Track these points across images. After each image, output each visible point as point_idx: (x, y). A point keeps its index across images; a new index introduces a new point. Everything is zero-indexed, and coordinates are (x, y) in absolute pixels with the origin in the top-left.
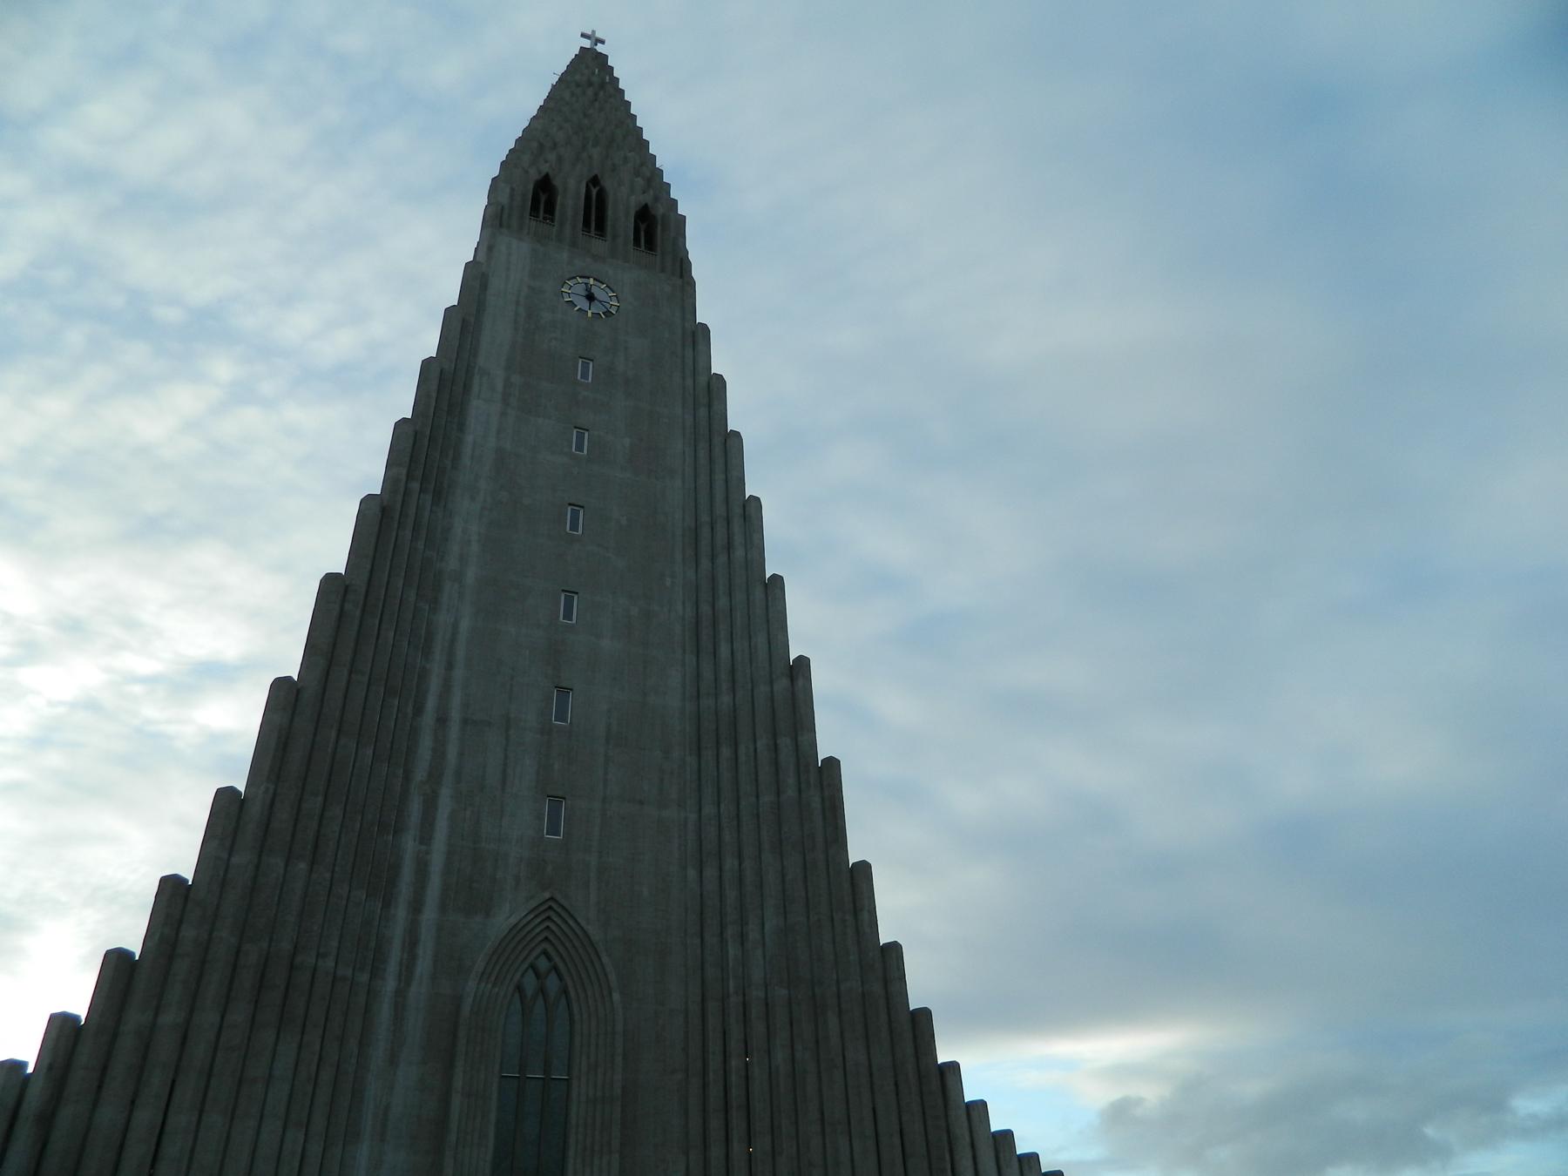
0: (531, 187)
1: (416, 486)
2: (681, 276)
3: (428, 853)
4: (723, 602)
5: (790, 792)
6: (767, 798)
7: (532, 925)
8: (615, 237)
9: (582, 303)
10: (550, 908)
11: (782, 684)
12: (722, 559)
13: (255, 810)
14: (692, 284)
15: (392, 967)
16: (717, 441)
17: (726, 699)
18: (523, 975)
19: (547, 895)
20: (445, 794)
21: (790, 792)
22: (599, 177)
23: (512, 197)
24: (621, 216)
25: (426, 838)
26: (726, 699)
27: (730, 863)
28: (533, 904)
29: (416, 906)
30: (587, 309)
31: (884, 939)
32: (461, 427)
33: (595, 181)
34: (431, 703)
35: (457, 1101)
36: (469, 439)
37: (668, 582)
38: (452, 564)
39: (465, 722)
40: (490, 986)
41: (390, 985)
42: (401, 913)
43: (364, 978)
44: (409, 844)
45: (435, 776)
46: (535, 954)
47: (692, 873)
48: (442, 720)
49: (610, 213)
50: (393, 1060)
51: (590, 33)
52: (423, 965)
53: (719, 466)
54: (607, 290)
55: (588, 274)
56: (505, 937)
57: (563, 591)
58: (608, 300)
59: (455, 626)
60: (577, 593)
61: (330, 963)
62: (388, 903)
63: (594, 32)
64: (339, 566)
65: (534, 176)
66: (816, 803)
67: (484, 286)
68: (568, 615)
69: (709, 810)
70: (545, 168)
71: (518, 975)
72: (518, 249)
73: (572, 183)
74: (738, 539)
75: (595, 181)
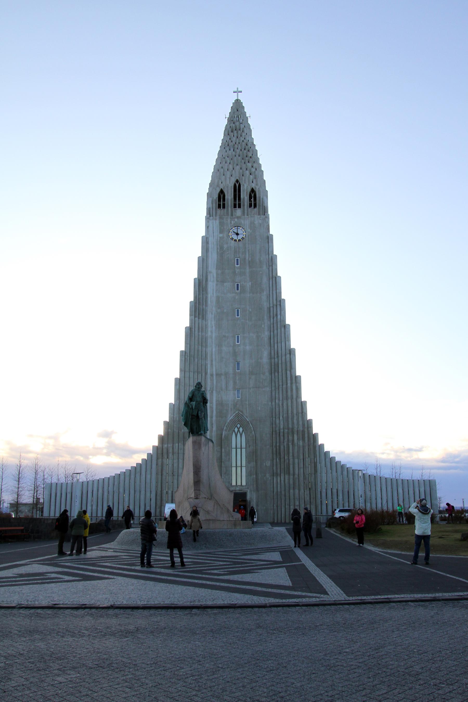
0: (217, 196)
1: (197, 319)
2: (264, 215)
3: (213, 405)
4: (275, 332)
5: (289, 385)
6: (284, 386)
8: (244, 205)
9: (235, 237)
11: (288, 356)
12: (275, 319)
13: (176, 406)
14: (267, 218)
16: (274, 279)
17: (276, 360)
18: (235, 429)
19: (237, 412)
20: (214, 392)
21: (289, 385)
23: (212, 204)
24: (245, 196)
26: (276, 360)
27: (277, 401)
28: (234, 414)
29: (212, 417)
30: (236, 239)
31: (308, 419)
32: (207, 293)
33: (237, 181)
35: (223, 454)
36: (209, 296)
37: (263, 326)
38: (209, 334)
39: (217, 375)
47: (270, 403)
48: (212, 375)
49: (242, 197)
52: (214, 429)
53: (274, 288)
54: (242, 229)
59: (212, 350)
63: (238, 88)
64: (183, 349)
65: (218, 190)
67: (207, 243)
68: (238, 342)
69: (273, 388)
70: (222, 186)
74: (279, 313)
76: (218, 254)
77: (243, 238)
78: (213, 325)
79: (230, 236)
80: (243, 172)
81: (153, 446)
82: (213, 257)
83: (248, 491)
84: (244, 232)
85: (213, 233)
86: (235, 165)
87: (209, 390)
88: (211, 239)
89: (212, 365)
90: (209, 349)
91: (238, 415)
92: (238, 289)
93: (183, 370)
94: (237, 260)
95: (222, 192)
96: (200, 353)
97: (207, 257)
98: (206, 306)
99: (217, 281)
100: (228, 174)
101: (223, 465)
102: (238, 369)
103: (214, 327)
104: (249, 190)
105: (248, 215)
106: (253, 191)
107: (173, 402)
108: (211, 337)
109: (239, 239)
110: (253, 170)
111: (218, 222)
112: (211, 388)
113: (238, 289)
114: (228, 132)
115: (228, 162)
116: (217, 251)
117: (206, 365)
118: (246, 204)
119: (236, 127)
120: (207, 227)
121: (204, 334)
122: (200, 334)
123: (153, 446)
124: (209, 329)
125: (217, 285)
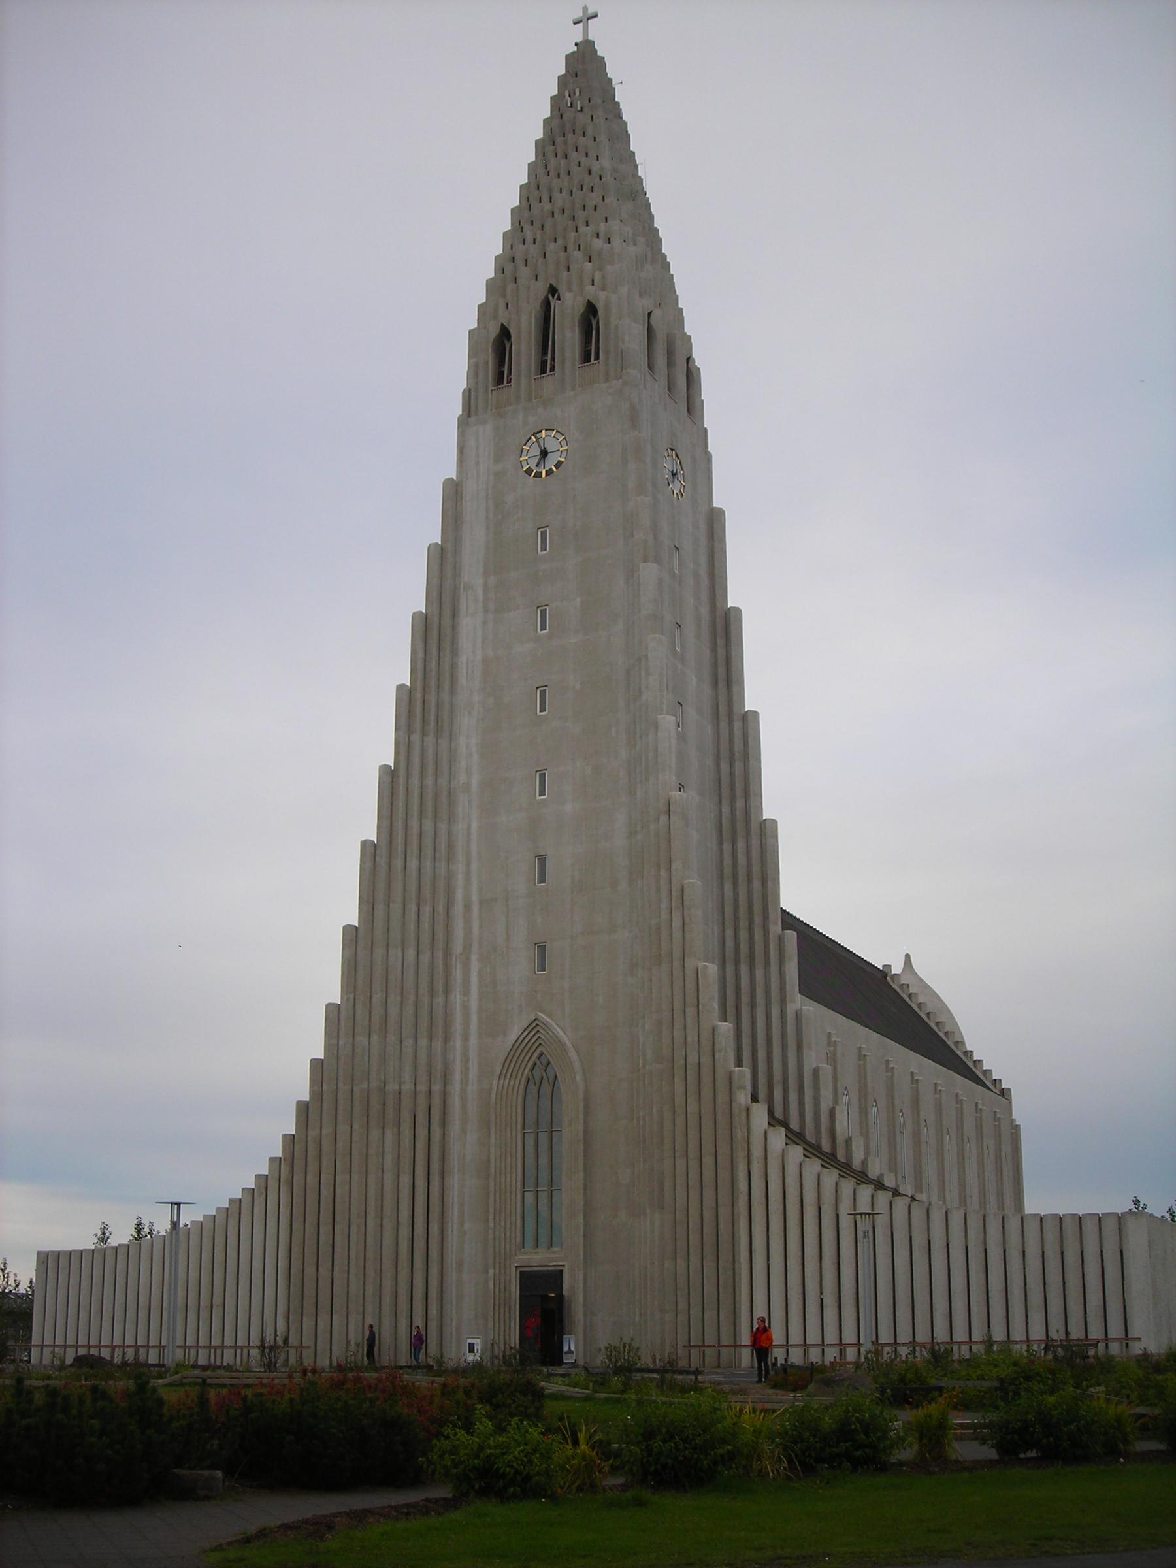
1: (416, 738)
3: (468, 1001)
7: (528, 1038)
10: (537, 1025)
15: (457, 1077)
20: (474, 957)
21: (664, 915)
22: (555, 286)
25: (466, 992)
29: (466, 1038)
32: (455, 652)
33: (553, 290)
34: (459, 894)
36: (463, 659)
38: (462, 778)
39: (481, 903)
40: (508, 1080)
41: (456, 1087)
42: (458, 1044)
43: (436, 1088)
44: (457, 997)
45: (467, 948)
46: (536, 1054)
48: (468, 907)
50: (464, 1131)
51: (579, 14)
54: (558, 435)
55: (540, 429)
56: (511, 1050)
57: (536, 772)
58: (557, 447)
60: (546, 770)
61: (407, 1087)
62: (447, 1039)
63: (585, 9)
65: (494, 332)
66: (677, 923)
68: (542, 793)
71: (526, 1071)
72: (485, 431)
73: (524, 318)
75: (553, 290)
76: (488, 528)
77: (558, 465)
78: (474, 749)
79: (524, 463)
80: (568, 258)
81: (285, 1136)
82: (476, 537)
83: (566, 1266)
84: (564, 443)
85: (477, 463)
86: (547, 242)
87: (461, 954)
88: (470, 487)
89: (468, 873)
90: (460, 827)
91: (535, 1026)
92: (543, 628)
93: (368, 900)
94: (544, 534)
95: (505, 334)
96: (428, 841)
97: (457, 540)
98: (453, 691)
99: (486, 611)
100: (524, 272)
101: (492, 1189)
102: (542, 879)
103: (475, 758)
104: (581, 308)
105: (573, 389)
106: (591, 310)
107: (337, 1000)
108: (467, 788)
109: (547, 469)
110: (598, 244)
111: (489, 428)
112: (465, 947)
113: (543, 628)
114: (543, 147)
115: (529, 239)
116: (487, 518)
117: (450, 878)
118: (568, 354)
119: (563, 126)
120: (461, 450)
121: (443, 782)
122: (429, 781)
123: (285, 1136)
124: (463, 764)
125: (485, 623)
